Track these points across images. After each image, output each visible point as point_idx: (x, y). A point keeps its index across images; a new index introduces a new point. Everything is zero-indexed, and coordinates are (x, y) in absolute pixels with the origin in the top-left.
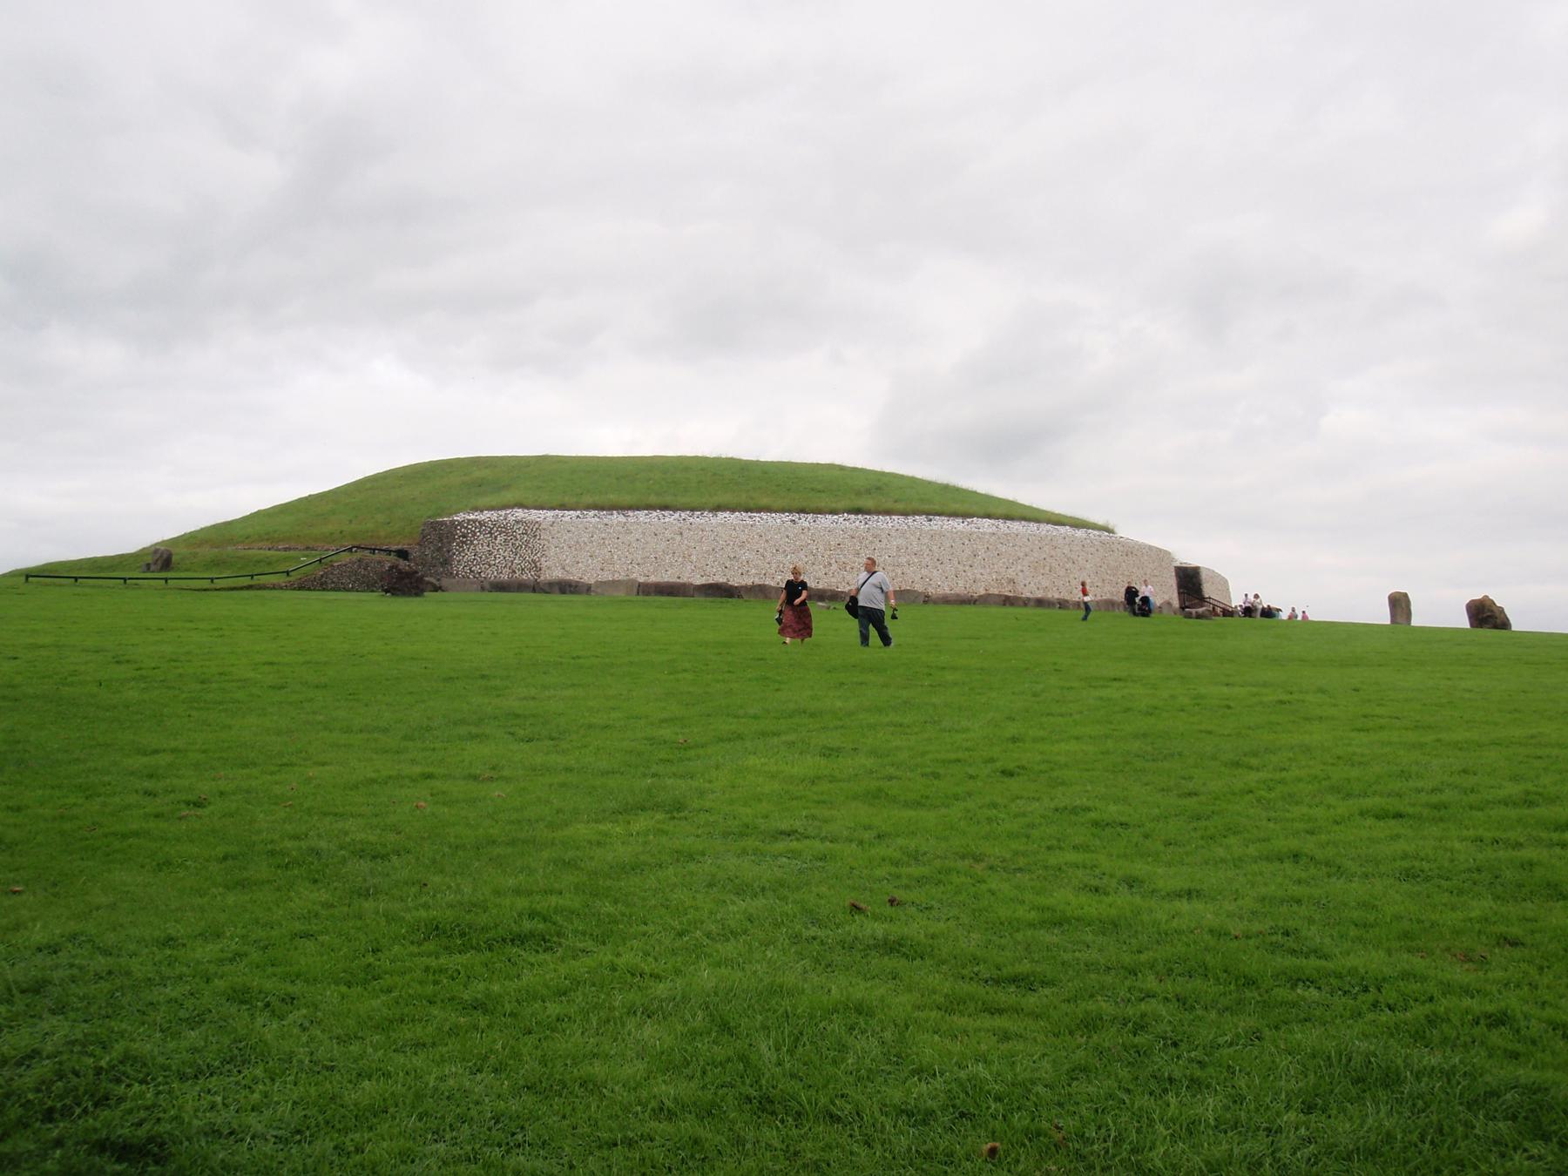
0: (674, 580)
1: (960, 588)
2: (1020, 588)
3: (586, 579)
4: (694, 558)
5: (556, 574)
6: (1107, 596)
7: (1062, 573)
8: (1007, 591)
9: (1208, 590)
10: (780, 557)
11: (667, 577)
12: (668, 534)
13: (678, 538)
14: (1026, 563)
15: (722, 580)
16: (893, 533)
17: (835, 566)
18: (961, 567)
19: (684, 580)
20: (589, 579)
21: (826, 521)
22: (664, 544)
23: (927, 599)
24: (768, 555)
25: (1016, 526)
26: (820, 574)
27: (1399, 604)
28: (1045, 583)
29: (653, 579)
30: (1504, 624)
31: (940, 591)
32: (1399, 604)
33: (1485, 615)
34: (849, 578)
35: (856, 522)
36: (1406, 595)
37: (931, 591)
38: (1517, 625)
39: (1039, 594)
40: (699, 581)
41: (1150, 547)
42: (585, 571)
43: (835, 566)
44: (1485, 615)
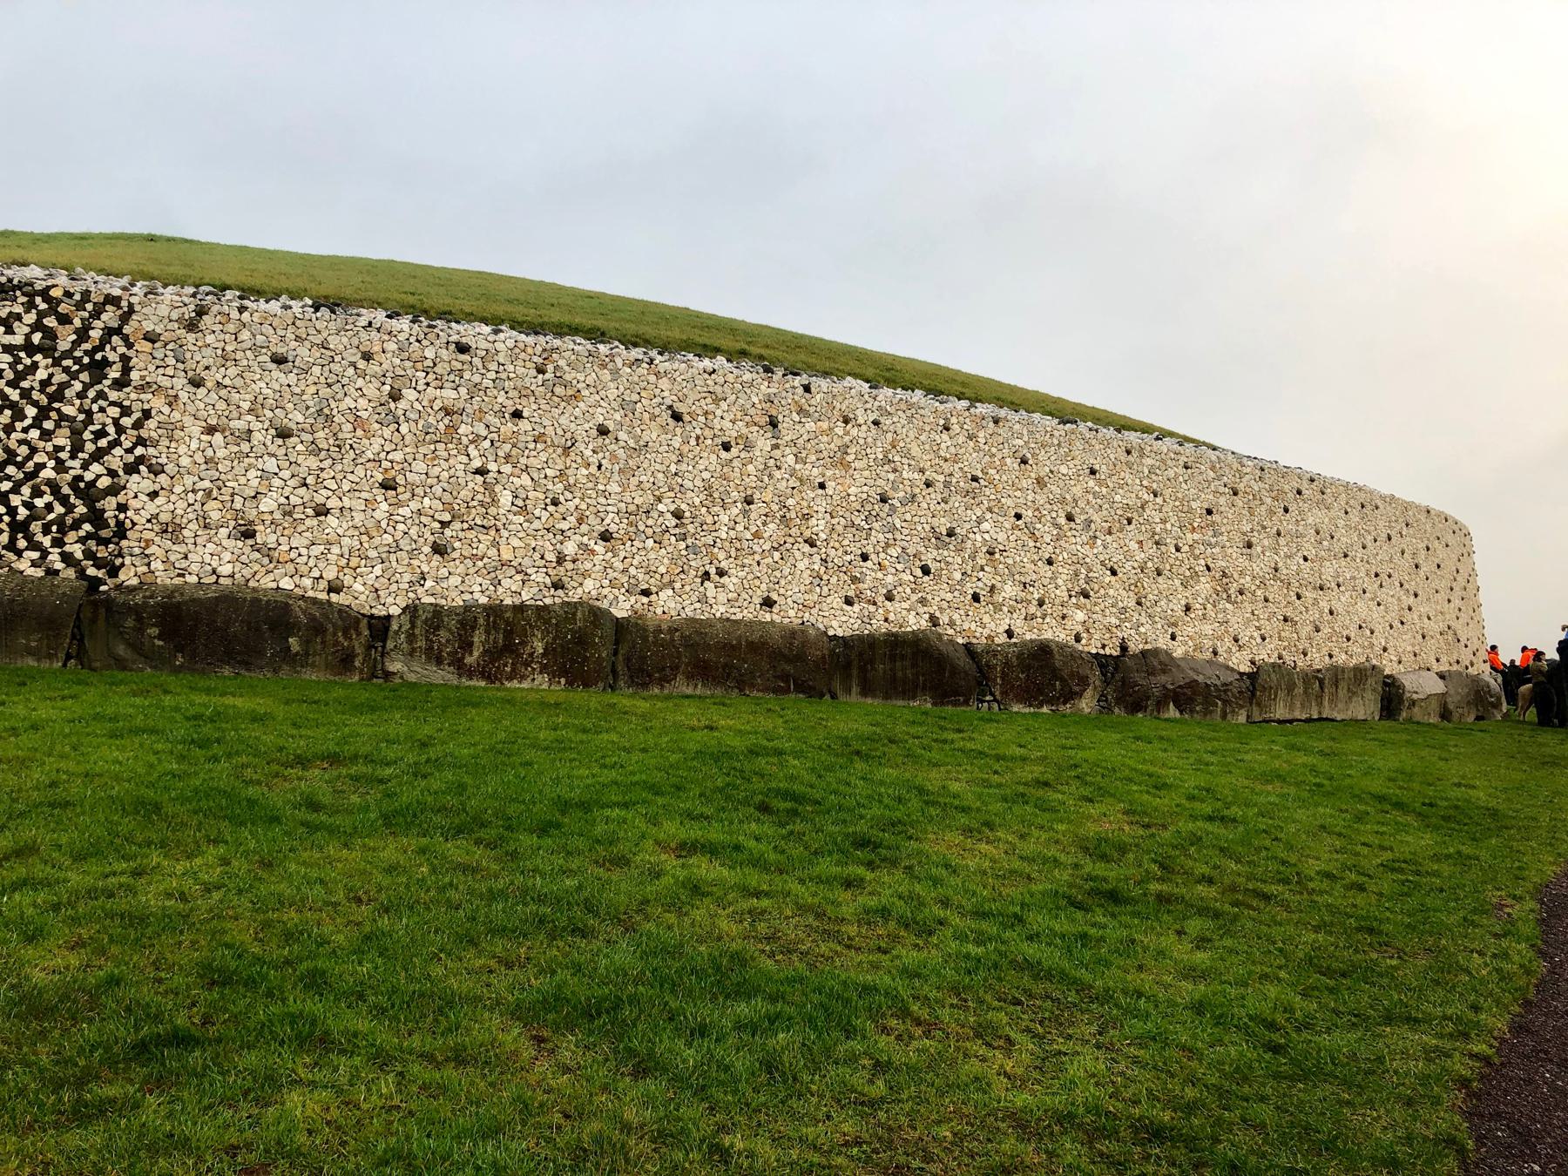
0: (749, 612)
3: (359, 595)
4: (819, 525)
5: (213, 562)
10: (1076, 543)
11: (726, 603)
12: (727, 424)
13: (763, 443)
15: (916, 622)
19: (787, 614)
20: (375, 591)
22: (711, 460)
24: (1046, 531)
29: (668, 606)
40: (841, 622)
42: (359, 555)
43: (1205, 586)
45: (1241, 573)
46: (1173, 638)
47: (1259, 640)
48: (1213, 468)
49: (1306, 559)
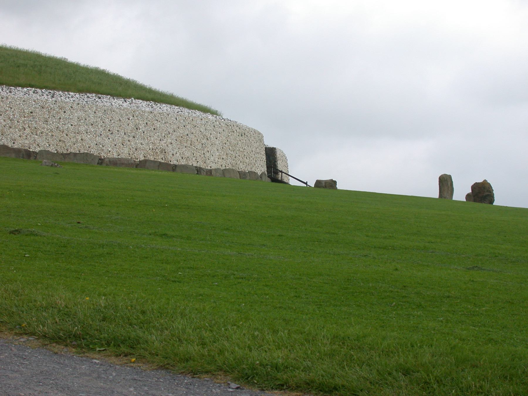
1: (125, 153)
2: (169, 157)
6: (230, 166)
7: (199, 147)
8: (160, 158)
9: (280, 166)
14: (174, 137)
16: (75, 106)
17: (28, 131)
18: (126, 137)
21: (20, 93)
23: (101, 161)
25: (165, 108)
26: (16, 136)
27: (445, 183)
28: (187, 154)
30: (492, 201)
31: (110, 156)
32: (445, 183)
33: (482, 193)
34: (39, 140)
35: (43, 96)
36: (450, 177)
37: (103, 155)
38: (494, 204)
39: (183, 162)
41: (255, 131)
44: (482, 193)
45: (44, 128)
46: (14, 143)
47: (48, 145)
48: (35, 101)
49: (72, 125)
